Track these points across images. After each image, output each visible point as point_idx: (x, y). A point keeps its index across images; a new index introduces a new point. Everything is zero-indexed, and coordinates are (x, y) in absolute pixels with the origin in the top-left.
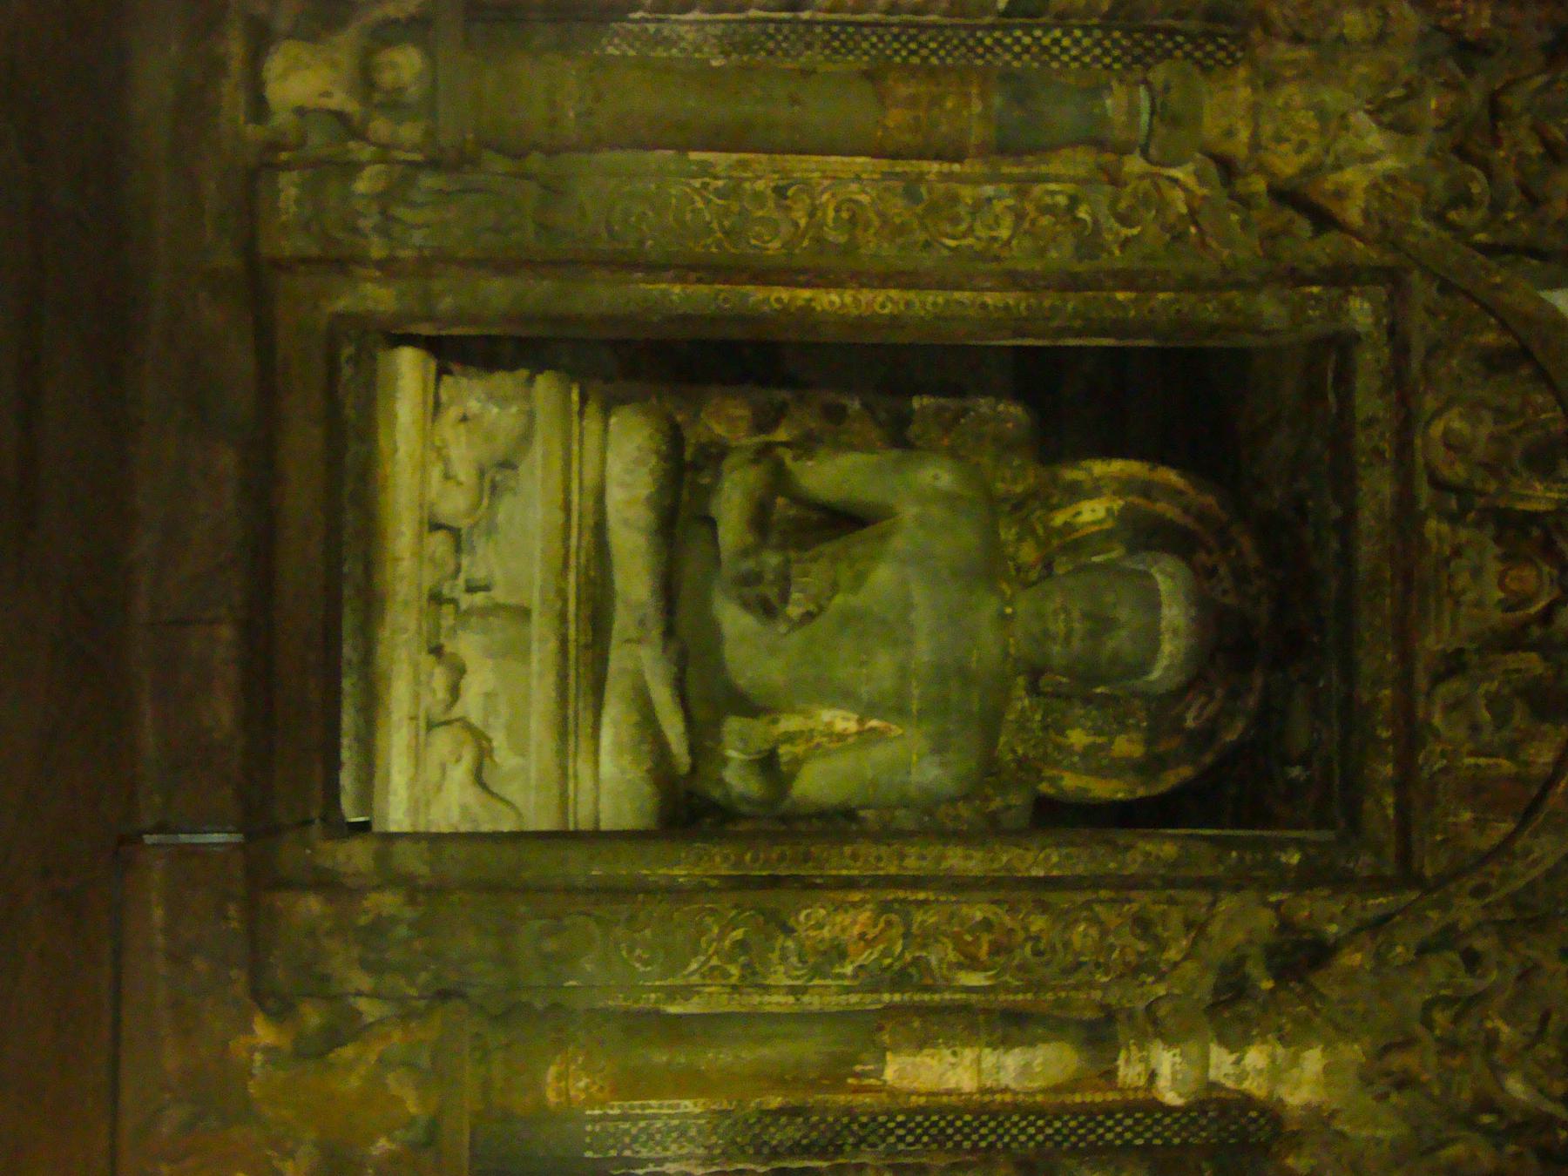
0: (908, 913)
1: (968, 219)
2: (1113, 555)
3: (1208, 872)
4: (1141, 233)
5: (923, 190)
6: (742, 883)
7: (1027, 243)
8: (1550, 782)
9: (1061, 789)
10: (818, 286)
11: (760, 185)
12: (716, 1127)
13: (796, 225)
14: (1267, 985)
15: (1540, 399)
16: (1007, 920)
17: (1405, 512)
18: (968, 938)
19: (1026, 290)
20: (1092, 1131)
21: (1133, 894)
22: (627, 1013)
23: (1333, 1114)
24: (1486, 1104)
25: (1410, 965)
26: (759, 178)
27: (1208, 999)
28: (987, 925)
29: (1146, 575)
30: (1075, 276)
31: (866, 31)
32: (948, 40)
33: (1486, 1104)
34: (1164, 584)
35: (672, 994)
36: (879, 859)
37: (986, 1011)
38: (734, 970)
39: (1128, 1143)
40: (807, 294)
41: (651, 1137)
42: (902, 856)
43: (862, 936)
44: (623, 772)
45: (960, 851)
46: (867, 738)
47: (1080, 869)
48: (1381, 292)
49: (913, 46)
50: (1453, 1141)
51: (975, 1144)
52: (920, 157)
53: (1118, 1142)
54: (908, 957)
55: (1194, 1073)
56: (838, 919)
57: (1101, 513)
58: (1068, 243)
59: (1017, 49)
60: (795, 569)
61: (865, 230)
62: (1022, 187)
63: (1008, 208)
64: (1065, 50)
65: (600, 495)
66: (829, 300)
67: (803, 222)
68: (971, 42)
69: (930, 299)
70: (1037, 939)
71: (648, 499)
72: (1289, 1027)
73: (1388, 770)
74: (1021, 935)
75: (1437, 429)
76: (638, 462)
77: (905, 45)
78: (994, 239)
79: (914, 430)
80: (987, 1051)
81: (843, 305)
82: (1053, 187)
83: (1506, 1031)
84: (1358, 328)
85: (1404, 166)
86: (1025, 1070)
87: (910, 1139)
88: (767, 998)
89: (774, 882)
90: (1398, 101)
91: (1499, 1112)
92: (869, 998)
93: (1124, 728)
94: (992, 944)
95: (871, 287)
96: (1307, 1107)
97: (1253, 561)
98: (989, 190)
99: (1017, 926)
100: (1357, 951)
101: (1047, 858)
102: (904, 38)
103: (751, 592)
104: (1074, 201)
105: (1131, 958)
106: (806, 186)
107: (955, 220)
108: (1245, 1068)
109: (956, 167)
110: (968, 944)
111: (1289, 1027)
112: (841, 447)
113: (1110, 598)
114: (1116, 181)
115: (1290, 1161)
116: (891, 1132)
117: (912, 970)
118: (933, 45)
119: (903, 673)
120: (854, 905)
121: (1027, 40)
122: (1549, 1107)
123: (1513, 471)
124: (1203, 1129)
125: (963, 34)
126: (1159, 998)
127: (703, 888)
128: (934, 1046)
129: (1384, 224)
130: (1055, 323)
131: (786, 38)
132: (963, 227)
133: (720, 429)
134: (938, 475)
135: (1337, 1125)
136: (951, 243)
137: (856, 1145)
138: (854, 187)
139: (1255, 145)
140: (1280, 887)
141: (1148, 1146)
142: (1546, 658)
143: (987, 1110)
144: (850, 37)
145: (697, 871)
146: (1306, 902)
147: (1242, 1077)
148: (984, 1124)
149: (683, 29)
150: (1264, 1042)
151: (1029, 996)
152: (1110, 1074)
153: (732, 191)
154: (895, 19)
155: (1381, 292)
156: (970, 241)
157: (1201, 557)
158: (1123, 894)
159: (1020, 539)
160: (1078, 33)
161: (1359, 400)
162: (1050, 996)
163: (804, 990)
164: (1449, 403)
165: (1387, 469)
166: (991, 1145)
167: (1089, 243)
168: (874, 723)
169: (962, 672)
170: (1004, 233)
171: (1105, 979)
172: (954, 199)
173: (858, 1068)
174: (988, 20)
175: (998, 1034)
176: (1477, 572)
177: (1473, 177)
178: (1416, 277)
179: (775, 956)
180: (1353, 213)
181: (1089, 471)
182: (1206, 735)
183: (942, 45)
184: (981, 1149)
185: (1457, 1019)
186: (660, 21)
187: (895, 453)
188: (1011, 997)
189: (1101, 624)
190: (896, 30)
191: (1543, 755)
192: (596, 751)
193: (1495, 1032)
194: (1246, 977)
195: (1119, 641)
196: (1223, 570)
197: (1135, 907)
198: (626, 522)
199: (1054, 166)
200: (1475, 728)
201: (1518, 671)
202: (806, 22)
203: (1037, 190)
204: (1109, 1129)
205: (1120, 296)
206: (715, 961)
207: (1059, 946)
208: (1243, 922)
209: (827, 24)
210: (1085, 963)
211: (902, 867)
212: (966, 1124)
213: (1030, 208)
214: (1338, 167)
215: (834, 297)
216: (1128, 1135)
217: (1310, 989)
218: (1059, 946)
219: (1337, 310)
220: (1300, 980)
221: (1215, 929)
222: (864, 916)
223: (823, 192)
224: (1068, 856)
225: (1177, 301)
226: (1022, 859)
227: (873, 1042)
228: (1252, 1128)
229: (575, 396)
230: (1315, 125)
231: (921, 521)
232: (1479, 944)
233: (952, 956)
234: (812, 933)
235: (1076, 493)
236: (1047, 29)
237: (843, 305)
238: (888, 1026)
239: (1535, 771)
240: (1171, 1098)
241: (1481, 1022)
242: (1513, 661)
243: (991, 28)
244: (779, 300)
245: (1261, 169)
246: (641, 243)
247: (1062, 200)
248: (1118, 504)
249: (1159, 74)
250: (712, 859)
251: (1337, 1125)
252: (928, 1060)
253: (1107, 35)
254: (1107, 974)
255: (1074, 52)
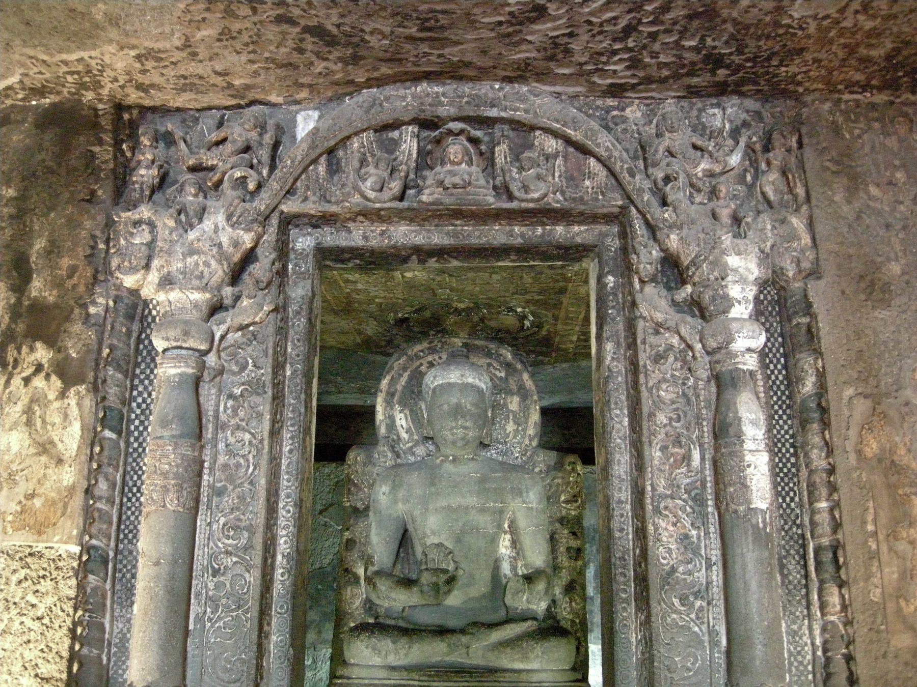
0: (660, 496)
1: (237, 458)
2: (423, 407)
3: (621, 327)
4: (251, 357)
5: (219, 485)
6: (643, 599)
7: (254, 423)
8: (568, 141)
9: (535, 436)
10: (275, 549)
11: (211, 585)
12: (791, 613)
13: (235, 563)
14: (689, 289)
15: (356, 145)
16: (661, 436)
17: (420, 216)
18: (672, 460)
19: (282, 426)
20: (778, 387)
21: (641, 363)
22: (729, 670)
23: (762, 252)
24: (741, 179)
25: (675, 210)
26: (206, 586)
27: (700, 321)
28: (664, 449)
29: (434, 389)
30: (274, 398)
31: (124, 517)
32: (133, 469)
33: (741, 179)
34: (439, 381)
35: (714, 643)
36: (622, 515)
37: (717, 449)
38: (698, 603)
39: (785, 367)
40: (279, 558)
41: (799, 653)
42: (620, 502)
43: (675, 525)
44: (537, 656)
45: (616, 467)
46: (514, 530)
47: (623, 398)
48: (293, 232)
49: (135, 490)
50: (763, 194)
51: (792, 455)
52: (199, 486)
53: (784, 372)
54: (685, 496)
55: (748, 324)
56: (665, 539)
57: (402, 415)
58: (255, 399)
59: (141, 428)
60: (431, 566)
61: (240, 520)
62: (220, 426)
63: (232, 434)
64: (144, 401)
65: (393, 668)
66: (284, 545)
67: (235, 559)
68: (135, 455)
69: (285, 483)
70: (671, 419)
71: (394, 642)
72: (716, 274)
73: (560, 229)
74: (668, 428)
75: (371, 195)
76: (374, 649)
77: (134, 495)
78: (250, 442)
79: (359, 505)
80: (745, 446)
81: (287, 536)
82: (222, 409)
83: (704, 165)
84: (313, 244)
85: (222, 211)
86: (754, 423)
87: (792, 494)
88: (715, 583)
89: (642, 580)
90: (187, 216)
91: (745, 171)
92: (711, 520)
93: (505, 405)
94: (674, 446)
95: (276, 518)
96: (759, 265)
97: (425, 345)
98: (221, 446)
99: (663, 431)
100: (668, 236)
101: (617, 416)
102: (130, 495)
103: (444, 589)
104: (231, 396)
105: (679, 365)
106: (213, 556)
107: (238, 465)
108: (741, 297)
109: (206, 465)
110: (675, 461)
111: (716, 274)
112: (368, 543)
113: (446, 407)
114: (221, 372)
115: (791, 274)
116: (788, 505)
117: (693, 494)
118: (135, 478)
119: (483, 510)
120: (656, 529)
121: (137, 422)
122: (742, 144)
123: (395, 159)
124: (771, 325)
125: (130, 460)
126: (703, 346)
127: (647, 623)
128: (745, 478)
129: (254, 221)
130: (303, 410)
131: (125, 566)
132: (242, 461)
133: (357, 602)
134: (382, 493)
135: (768, 250)
136: (251, 468)
137: (798, 527)
138: (215, 527)
139: (204, 288)
140: (631, 284)
141: (785, 355)
142: (499, 143)
143: (773, 447)
144: (127, 527)
145: (633, 627)
146: (642, 266)
147: (747, 301)
148: (780, 450)
149: (116, 631)
150: (726, 286)
151: (705, 423)
152: (752, 373)
153: (214, 601)
154: (117, 500)
155: (293, 232)
156: (250, 457)
157: (423, 368)
158: (641, 369)
159: (414, 454)
160: (135, 393)
161: (353, 244)
162: (704, 411)
163: (708, 559)
164: (356, 188)
165: (392, 228)
166: (793, 445)
167: (255, 387)
168: (506, 526)
169: (483, 480)
170: (247, 436)
171: (692, 380)
172: (226, 466)
173: (761, 525)
174: (122, 444)
175: (734, 440)
176: (453, 173)
177: (231, 176)
178: (284, 208)
179: (689, 579)
180: (247, 239)
181: (381, 421)
182: (508, 366)
183: (136, 473)
184: (796, 452)
185: (699, 191)
186: (110, 644)
187: (371, 514)
188: (706, 434)
189: (457, 411)
190: (125, 500)
191: (552, 144)
192: (528, 671)
193: (704, 170)
194: (685, 300)
195: (468, 402)
196: (430, 358)
197: (648, 362)
198: (406, 655)
199: (209, 406)
200: (539, 177)
201: (505, 158)
202: (116, 555)
203: (223, 417)
204: (777, 378)
205: (288, 373)
206: (693, 616)
207: (674, 406)
208: (654, 304)
209: (118, 541)
210: (683, 393)
211: (626, 502)
212: (780, 461)
213: (233, 422)
214: (220, 245)
215: (282, 541)
216: (779, 367)
217: (693, 262)
218: (674, 406)
219: (302, 255)
220: (688, 268)
221: (659, 317)
222: (662, 524)
223: (217, 546)
224: (616, 403)
225: (293, 341)
226: (619, 431)
227: (745, 516)
228: (769, 298)
229: (339, 681)
230: (196, 257)
231: (406, 501)
232: (660, 175)
233: (684, 470)
234: (674, 556)
235: (391, 426)
236: (131, 410)
237: (287, 536)
238: (734, 507)
239: (561, 148)
240: (763, 339)
241: (700, 179)
242: (500, 160)
243: (128, 444)
244: (282, 575)
245: (219, 288)
246: (243, 662)
247: (230, 403)
248: (397, 407)
249: (159, 344)
250: (625, 619)
251: (768, 250)
252: (754, 482)
253: (134, 376)
254: (688, 379)
255: (146, 395)
